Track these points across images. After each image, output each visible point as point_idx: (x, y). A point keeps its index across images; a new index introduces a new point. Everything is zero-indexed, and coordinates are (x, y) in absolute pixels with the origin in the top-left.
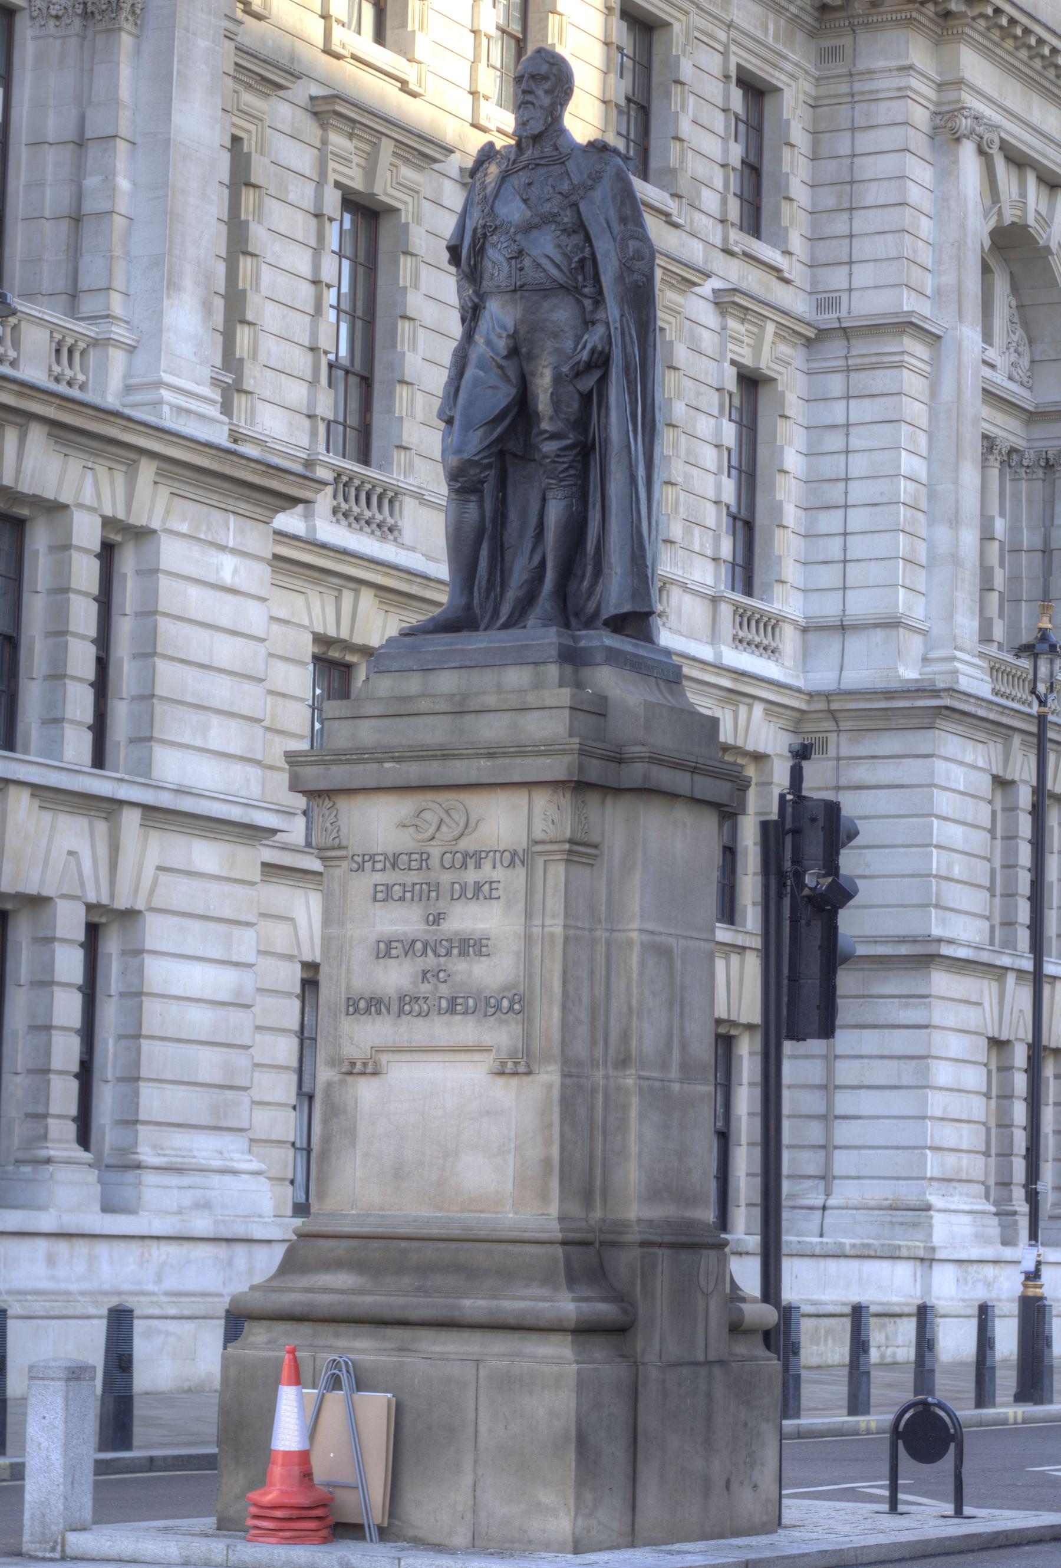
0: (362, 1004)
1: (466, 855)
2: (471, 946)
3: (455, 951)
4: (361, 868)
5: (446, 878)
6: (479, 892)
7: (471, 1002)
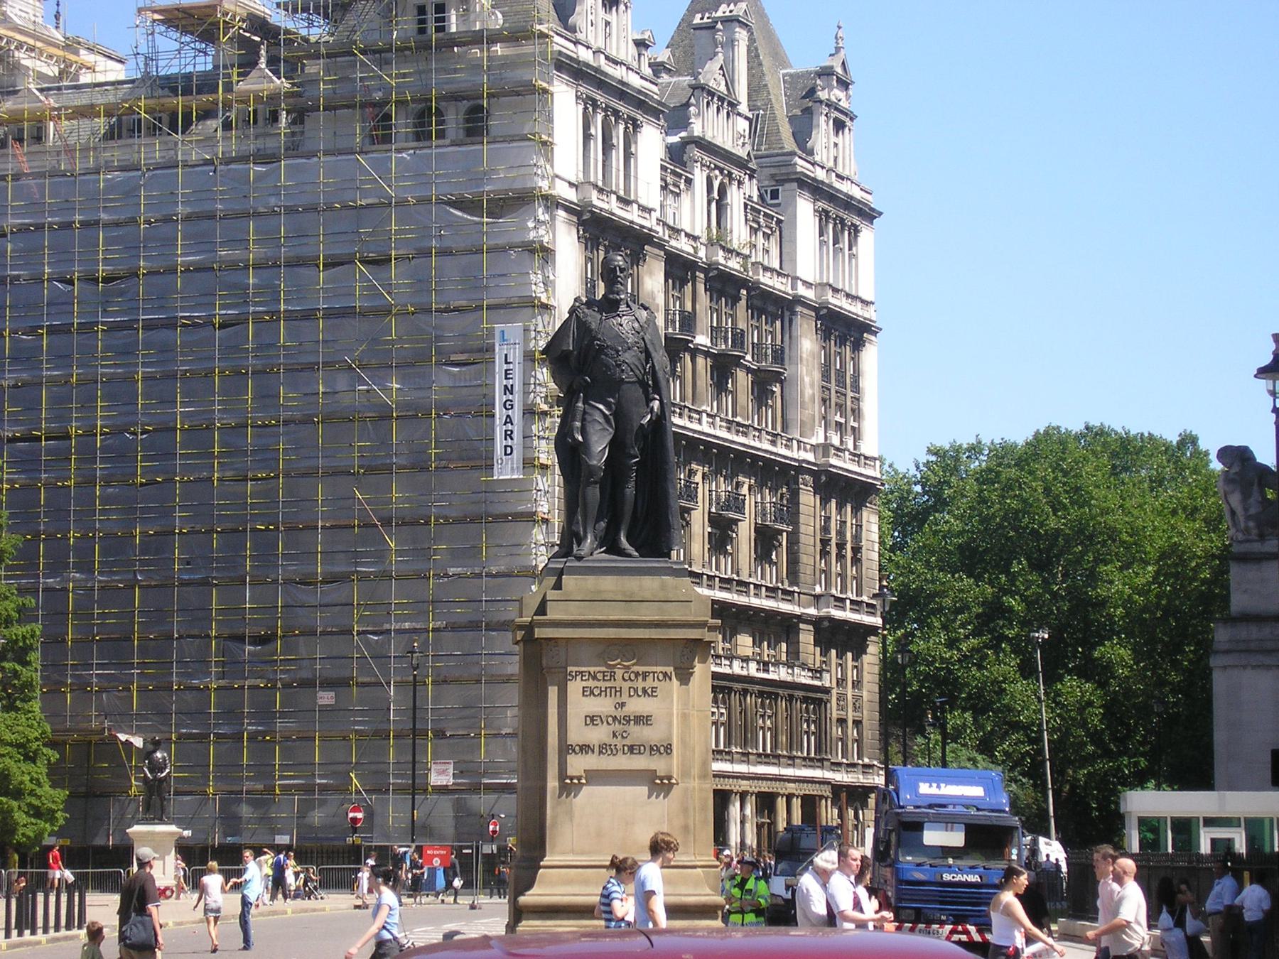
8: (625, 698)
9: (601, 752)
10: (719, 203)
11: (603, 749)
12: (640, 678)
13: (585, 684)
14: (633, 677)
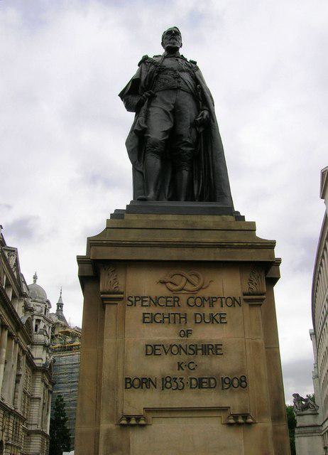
0: (136, 382)
1: (203, 299)
2: (212, 349)
3: (200, 352)
4: (134, 304)
5: (191, 312)
7: (212, 381)
8: (190, 326)
9: (164, 387)
11: (168, 383)
12: (207, 304)
13: (145, 310)
14: (199, 301)
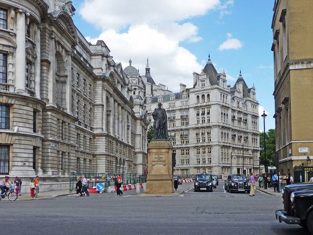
2: (161, 158)
6: (162, 155)
10: (238, 103)
